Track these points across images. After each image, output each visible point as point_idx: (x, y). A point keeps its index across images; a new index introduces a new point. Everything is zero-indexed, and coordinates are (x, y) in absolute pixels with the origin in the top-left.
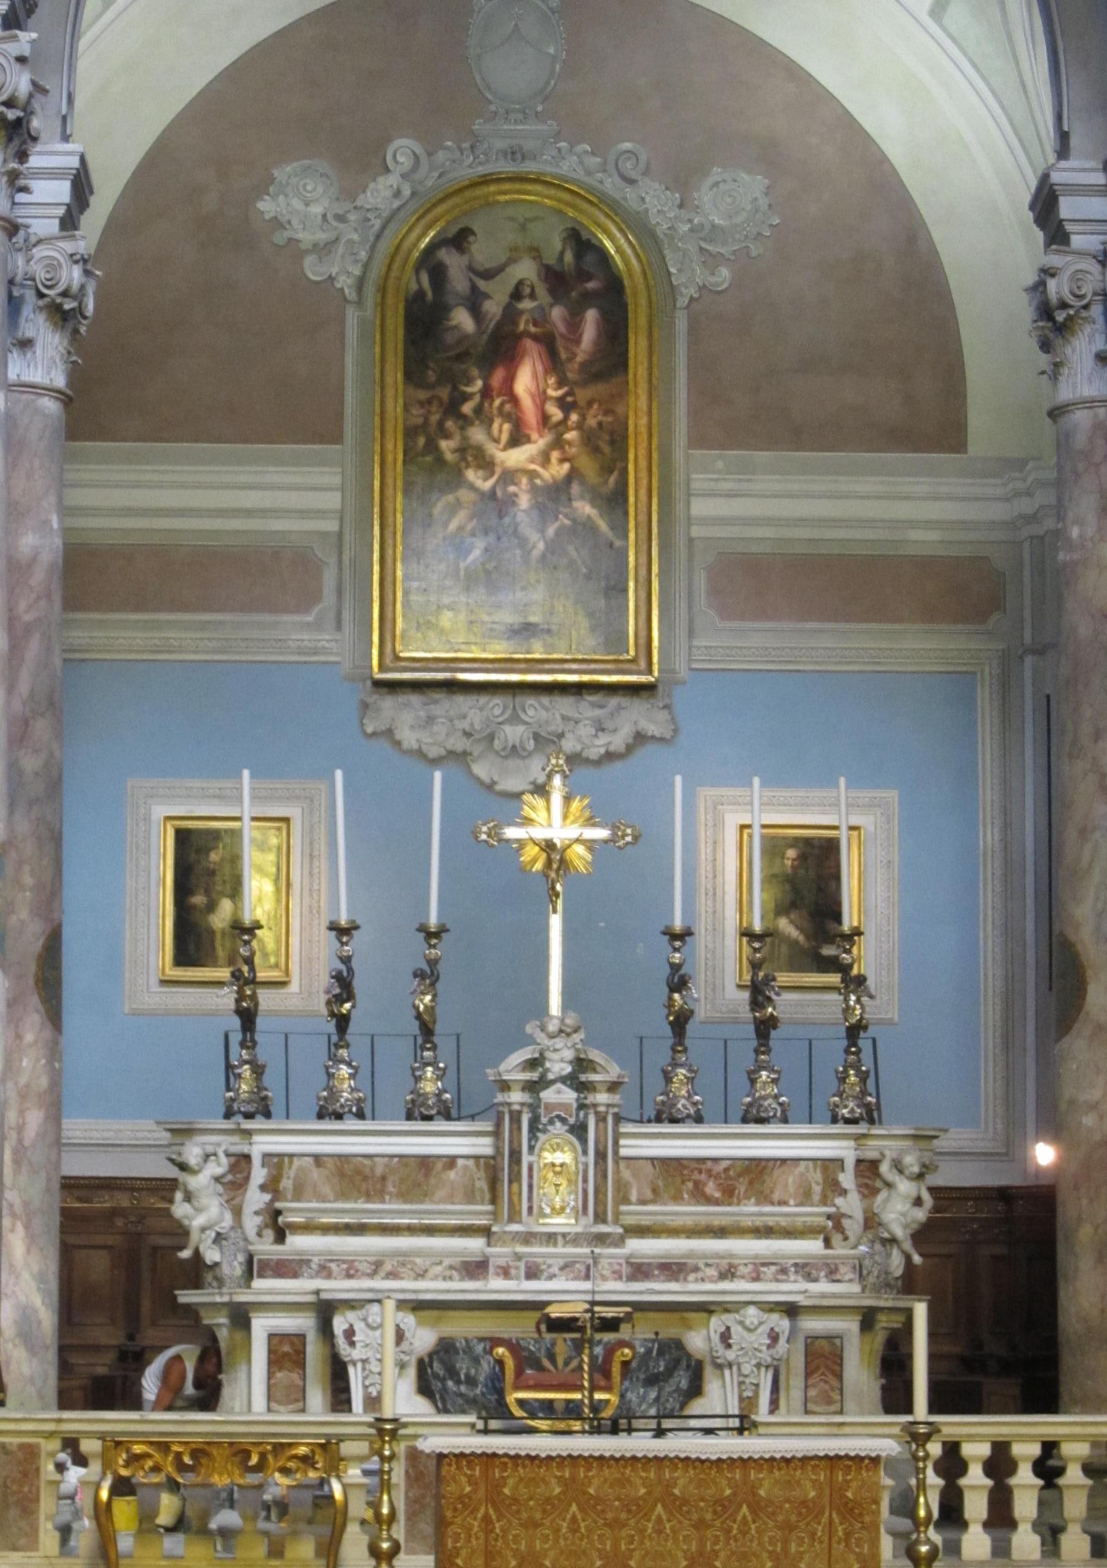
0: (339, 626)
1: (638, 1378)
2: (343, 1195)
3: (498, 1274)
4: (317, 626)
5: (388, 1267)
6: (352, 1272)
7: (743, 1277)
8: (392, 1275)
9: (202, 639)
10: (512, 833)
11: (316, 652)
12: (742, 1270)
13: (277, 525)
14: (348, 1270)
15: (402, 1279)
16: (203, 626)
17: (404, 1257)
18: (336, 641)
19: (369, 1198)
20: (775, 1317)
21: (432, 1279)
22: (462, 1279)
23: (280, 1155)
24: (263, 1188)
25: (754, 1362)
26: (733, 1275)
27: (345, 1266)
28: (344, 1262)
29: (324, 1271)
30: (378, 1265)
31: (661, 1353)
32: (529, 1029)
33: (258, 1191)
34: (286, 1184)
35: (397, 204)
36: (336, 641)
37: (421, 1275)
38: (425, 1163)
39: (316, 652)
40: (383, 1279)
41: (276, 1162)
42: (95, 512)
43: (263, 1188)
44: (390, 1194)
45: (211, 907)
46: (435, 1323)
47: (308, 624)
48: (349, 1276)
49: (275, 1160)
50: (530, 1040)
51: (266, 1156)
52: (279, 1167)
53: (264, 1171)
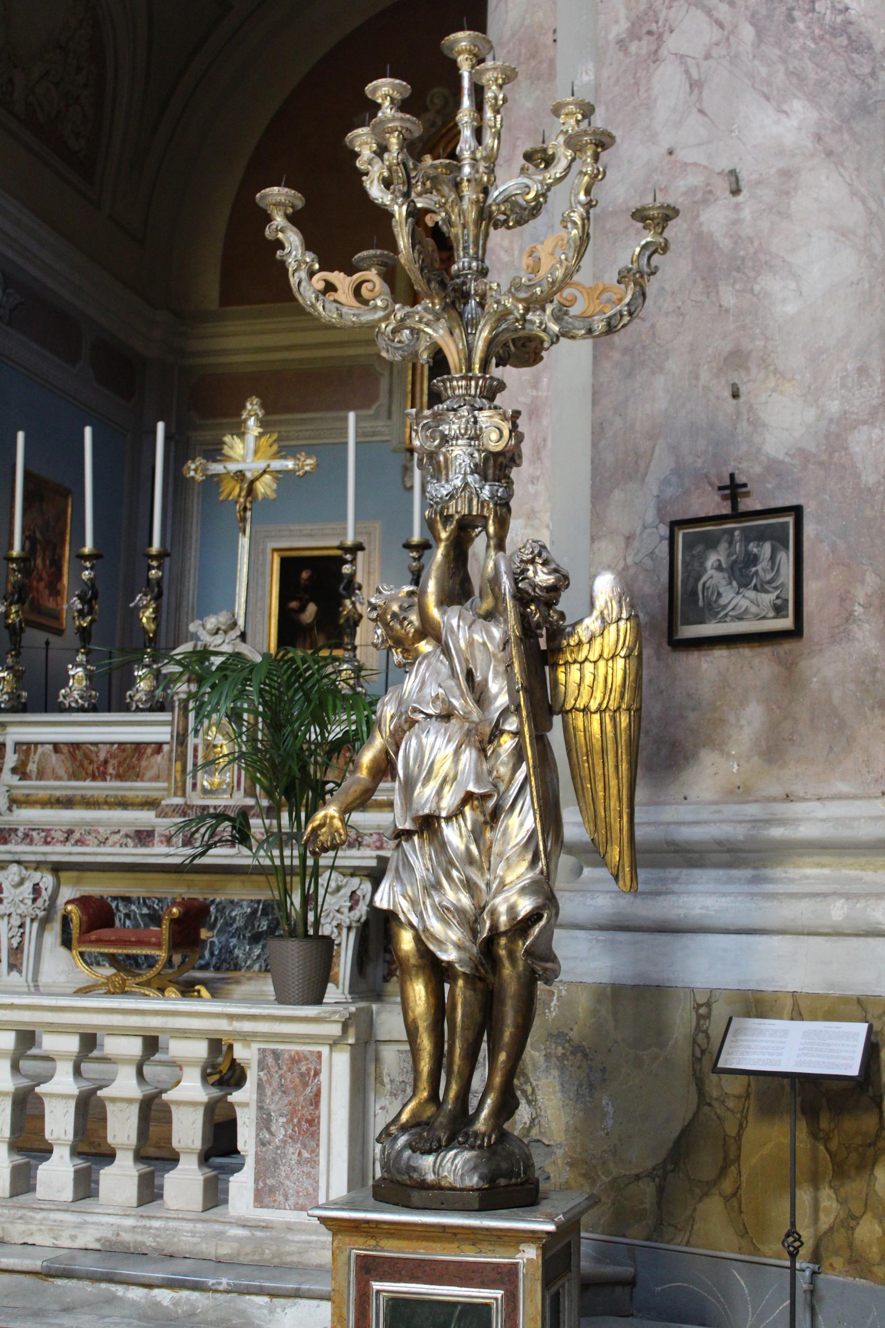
0: (390, 417)
1: (244, 936)
2: (74, 776)
3: (162, 842)
4: (376, 417)
5: (77, 835)
6: (49, 839)
7: (368, 846)
8: (80, 842)
9: (301, 431)
10: (216, 468)
11: (374, 434)
12: (367, 840)
13: (351, 351)
14: (46, 837)
15: (88, 845)
16: (303, 421)
17: (91, 828)
18: (388, 426)
19: (94, 778)
20: (356, 881)
21: (111, 846)
22: (135, 846)
23: (28, 744)
24: (14, 771)
25: (335, 923)
26: (360, 844)
27: (43, 834)
28: (43, 830)
29: (27, 838)
30: (70, 832)
31: (265, 913)
32: (192, 627)
33: (9, 773)
34: (32, 767)
35: (433, 130)
36: (388, 426)
37: (103, 842)
38: (139, 747)
39: (374, 434)
40: (73, 845)
41: (25, 748)
42: (237, 351)
43: (14, 771)
44: (111, 775)
45: (303, 609)
46: (77, 882)
47: (371, 416)
48: (47, 843)
49: (24, 747)
50: (195, 637)
51: (17, 744)
52: (28, 751)
53: (15, 757)
